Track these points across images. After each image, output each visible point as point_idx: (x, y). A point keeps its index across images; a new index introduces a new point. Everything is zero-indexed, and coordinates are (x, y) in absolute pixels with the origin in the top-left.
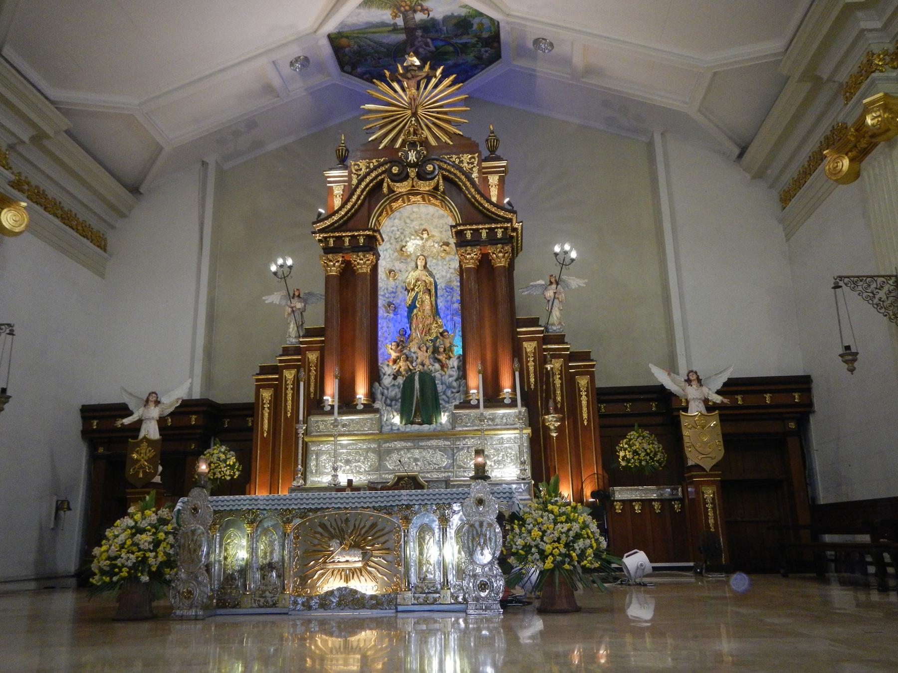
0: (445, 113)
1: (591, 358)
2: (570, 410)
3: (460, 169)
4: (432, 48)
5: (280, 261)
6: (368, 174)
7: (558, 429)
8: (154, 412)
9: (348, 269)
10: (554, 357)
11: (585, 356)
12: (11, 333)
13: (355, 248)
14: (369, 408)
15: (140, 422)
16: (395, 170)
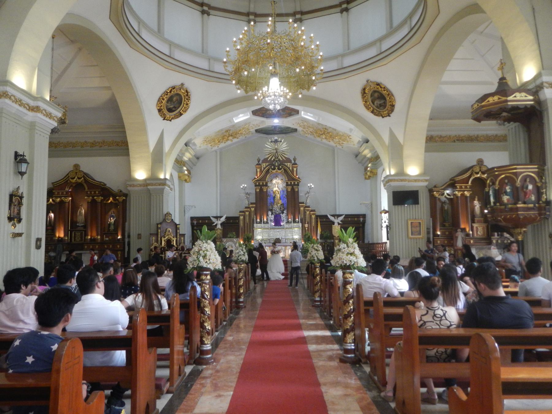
0: (284, 152)
1: (316, 211)
2: (310, 223)
3: (287, 166)
4: (280, 130)
5: (243, 185)
6: (266, 167)
7: (308, 228)
8: (219, 222)
9: (261, 190)
10: (307, 211)
11: (314, 211)
12: (195, 207)
13: (263, 185)
14: (267, 223)
15: (216, 225)
16: (272, 167)
